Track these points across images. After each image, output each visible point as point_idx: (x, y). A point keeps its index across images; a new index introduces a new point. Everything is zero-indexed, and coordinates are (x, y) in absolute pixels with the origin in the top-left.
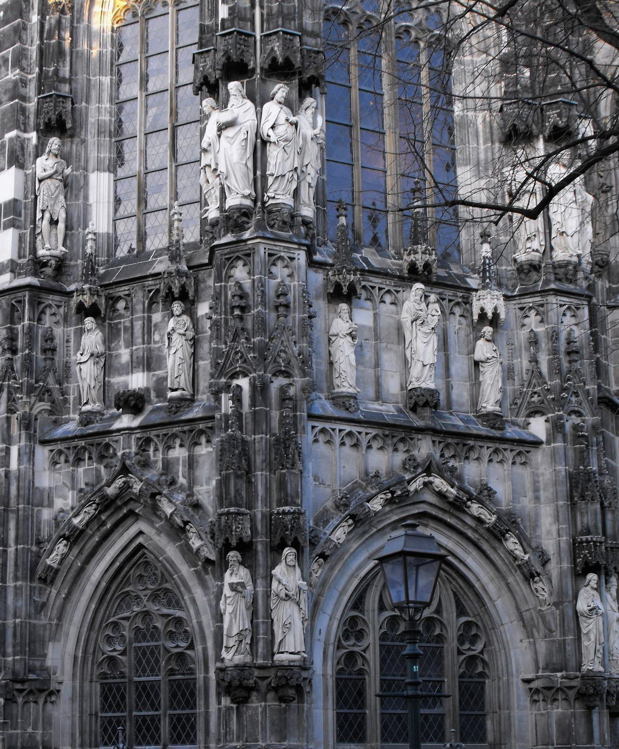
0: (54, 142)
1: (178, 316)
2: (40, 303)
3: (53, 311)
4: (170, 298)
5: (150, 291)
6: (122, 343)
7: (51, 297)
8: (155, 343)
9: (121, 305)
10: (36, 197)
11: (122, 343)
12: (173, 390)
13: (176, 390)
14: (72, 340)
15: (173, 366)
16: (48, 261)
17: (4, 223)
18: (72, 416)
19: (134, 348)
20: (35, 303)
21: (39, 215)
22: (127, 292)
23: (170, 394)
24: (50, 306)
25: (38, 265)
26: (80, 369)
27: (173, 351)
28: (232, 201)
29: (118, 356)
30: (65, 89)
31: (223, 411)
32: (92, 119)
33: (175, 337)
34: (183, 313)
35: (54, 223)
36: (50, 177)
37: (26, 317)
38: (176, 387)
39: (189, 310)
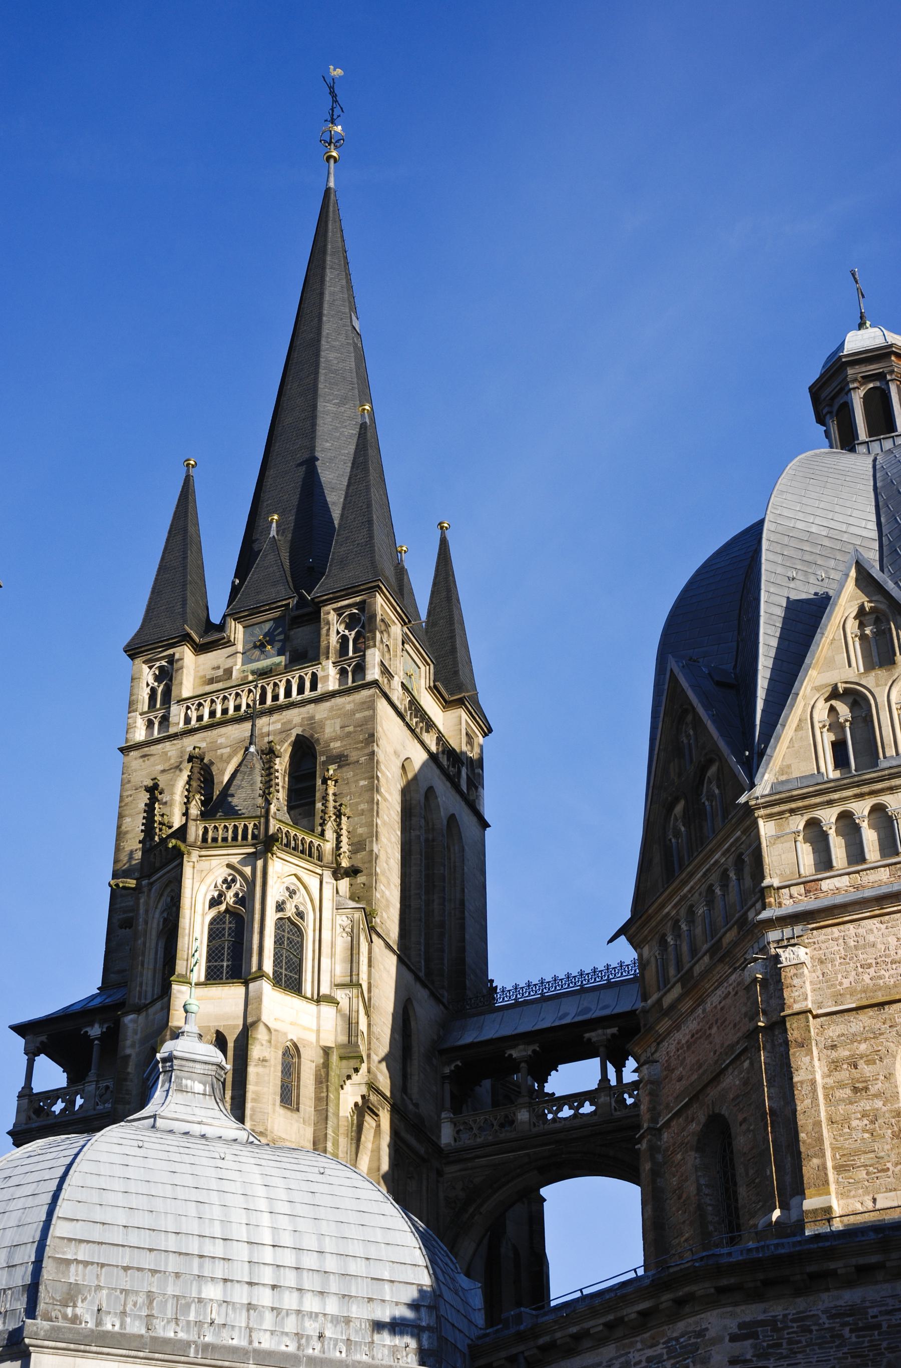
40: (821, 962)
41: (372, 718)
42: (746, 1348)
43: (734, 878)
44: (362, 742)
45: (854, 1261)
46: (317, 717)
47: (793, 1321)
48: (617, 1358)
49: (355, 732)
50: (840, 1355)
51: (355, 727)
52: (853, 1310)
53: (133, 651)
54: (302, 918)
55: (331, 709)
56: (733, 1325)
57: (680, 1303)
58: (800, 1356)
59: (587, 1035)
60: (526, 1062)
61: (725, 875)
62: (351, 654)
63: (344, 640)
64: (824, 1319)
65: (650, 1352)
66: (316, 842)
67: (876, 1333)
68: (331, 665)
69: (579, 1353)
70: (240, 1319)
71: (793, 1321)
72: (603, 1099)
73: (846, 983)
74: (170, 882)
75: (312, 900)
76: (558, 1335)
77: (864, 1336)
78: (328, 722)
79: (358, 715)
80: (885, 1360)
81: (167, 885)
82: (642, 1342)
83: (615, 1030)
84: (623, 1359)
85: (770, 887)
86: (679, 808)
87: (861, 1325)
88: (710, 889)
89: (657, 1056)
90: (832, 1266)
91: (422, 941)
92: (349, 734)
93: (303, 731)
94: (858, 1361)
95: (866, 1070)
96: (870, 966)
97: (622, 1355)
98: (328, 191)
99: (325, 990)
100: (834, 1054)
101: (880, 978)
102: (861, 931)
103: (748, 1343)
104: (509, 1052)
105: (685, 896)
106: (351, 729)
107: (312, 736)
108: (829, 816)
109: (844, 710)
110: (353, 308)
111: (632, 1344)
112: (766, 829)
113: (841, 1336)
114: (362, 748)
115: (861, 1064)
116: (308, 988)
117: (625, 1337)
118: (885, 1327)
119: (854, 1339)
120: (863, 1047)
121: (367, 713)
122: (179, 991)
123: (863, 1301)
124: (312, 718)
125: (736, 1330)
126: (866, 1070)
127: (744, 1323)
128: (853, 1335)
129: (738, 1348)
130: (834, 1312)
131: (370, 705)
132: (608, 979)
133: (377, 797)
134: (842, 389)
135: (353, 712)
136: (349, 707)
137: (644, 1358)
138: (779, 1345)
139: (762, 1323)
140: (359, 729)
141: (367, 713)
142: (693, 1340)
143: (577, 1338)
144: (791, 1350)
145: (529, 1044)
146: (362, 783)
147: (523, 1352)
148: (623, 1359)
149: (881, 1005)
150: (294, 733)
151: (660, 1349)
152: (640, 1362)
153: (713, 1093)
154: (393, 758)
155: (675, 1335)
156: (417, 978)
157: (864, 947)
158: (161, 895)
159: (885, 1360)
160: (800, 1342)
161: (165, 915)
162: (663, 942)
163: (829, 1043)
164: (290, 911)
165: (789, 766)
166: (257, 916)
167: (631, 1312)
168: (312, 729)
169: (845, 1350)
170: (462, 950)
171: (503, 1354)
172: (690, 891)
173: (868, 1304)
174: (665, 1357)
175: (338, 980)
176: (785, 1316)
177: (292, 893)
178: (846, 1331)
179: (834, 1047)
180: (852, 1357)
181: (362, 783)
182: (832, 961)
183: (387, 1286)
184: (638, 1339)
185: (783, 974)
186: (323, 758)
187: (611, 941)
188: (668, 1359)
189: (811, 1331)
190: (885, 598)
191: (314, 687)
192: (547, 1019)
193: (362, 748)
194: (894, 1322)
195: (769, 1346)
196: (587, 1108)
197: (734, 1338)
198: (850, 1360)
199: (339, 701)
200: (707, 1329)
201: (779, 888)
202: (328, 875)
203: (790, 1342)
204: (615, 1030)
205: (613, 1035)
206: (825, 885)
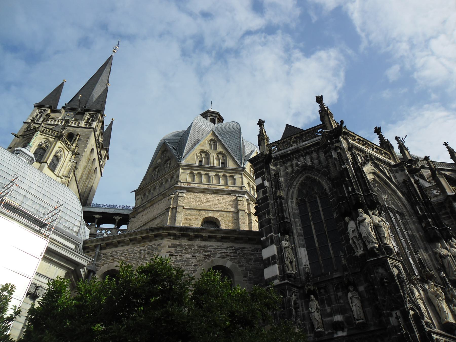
0: (287, 237)
1: (352, 291)
2: (291, 290)
3: (295, 294)
4: (349, 284)
5: (335, 285)
6: (326, 305)
7: (294, 288)
8: (341, 303)
9: (322, 291)
10: (283, 254)
11: (326, 305)
12: (357, 320)
13: (360, 320)
14: (304, 305)
15: (356, 310)
16: (292, 275)
17: (272, 263)
18: (309, 335)
19: (333, 306)
20: (290, 290)
21: (286, 260)
22: (325, 286)
23: (357, 322)
24: (294, 292)
25: (289, 276)
26: (312, 315)
27: (354, 304)
28: (370, 246)
29: (326, 310)
30: (286, 220)
31: (392, 324)
32: (295, 232)
33: (354, 299)
34: (354, 290)
35: (291, 262)
36: (288, 247)
37: (288, 295)
38: (360, 318)
39: (356, 289)
40: (188, 198)
41: (90, 134)
42: (173, 250)
43: (169, 181)
45: (208, 234)
46: (77, 130)
47: (187, 246)
48: (130, 249)
50: (199, 256)
52: (204, 246)
53: (36, 106)
54: (61, 158)
55: (81, 130)
56: (170, 244)
57: (156, 236)
58: (187, 254)
59: (114, 217)
60: (97, 219)
61: (167, 180)
62: (90, 122)
63: (89, 119)
64: (196, 247)
65: (141, 248)
66: (70, 145)
67: (210, 253)
68: (84, 122)
69: (118, 247)
70: (20, 198)
71: (187, 246)
72: (114, 231)
73: (193, 204)
74: (29, 138)
76: (114, 240)
77: (207, 253)
79: (87, 133)
80: (211, 260)
81: (27, 139)
82: (139, 246)
83: (121, 218)
84: (132, 249)
85: (180, 181)
86: (157, 170)
87: (206, 250)
88: (162, 184)
89: (135, 217)
90: (202, 234)
91: (82, 186)
94: (204, 258)
95: (194, 222)
96: (199, 202)
97: (132, 248)
98: (112, 56)
99: (60, 175)
100: (186, 217)
101: (201, 205)
102: (198, 195)
103: (173, 249)
104: (94, 216)
105: (154, 184)
107: (74, 133)
108: (196, 172)
109: (203, 155)
110: (110, 74)
111: (136, 246)
112: (181, 171)
113: (200, 252)
115: (192, 221)
116: (56, 172)
117: (135, 244)
118: (212, 252)
119: (203, 253)
120: (194, 217)
121: (89, 133)
123: (208, 245)
124: (76, 130)
125: (171, 245)
126: (194, 222)
127: (173, 244)
128: (203, 252)
129: (169, 249)
130: (199, 246)
131: (91, 132)
132: (122, 208)
133: (85, 149)
134: (207, 116)
135: (86, 132)
136: (85, 131)
137: (139, 249)
138: (183, 251)
139: (178, 245)
141: (89, 133)
142: (156, 246)
143: (119, 242)
144: (185, 252)
145: (99, 215)
146: (83, 145)
147: (100, 244)
148: (132, 249)
149: (200, 210)
150: (70, 132)
151: (145, 248)
152: (138, 250)
153: (150, 223)
154: (91, 146)
155: (151, 244)
156: (79, 192)
157: (198, 198)
158: (25, 140)
159: (211, 260)
160: (188, 251)
161: (24, 145)
162: (145, 195)
163: (186, 214)
164: (59, 154)
165: (189, 161)
166: (50, 151)
167: (139, 237)
169: (201, 255)
170: (89, 195)
171: (94, 244)
172: (156, 184)
173: (209, 246)
174: (146, 249)
175: (64, 175)
176: (185, 244)
177: (61, 152)
178: (201, 251)
179: (187, 215)
180: (202, 257)
181: (83, 145)
182: (191, 199)
183: (69, 211)
184: (139, 245)
185: (179, 198)
187: (131, 192)
188: (147, 250)
189: (192, 249)
190: (217, 138)
191: (78, 125)
192: (107, 211)
194: (215, 251)
195: (179, 250)
196: (109, 232)
197: (169, 247)
198: (201, 258)
199: (84, 129)
200: (162, 244)
201: (182, 182)
202: (70, 153)
203: (185, 250)
204: (121, 218)
205: (121, 218)
206: (192, 185)
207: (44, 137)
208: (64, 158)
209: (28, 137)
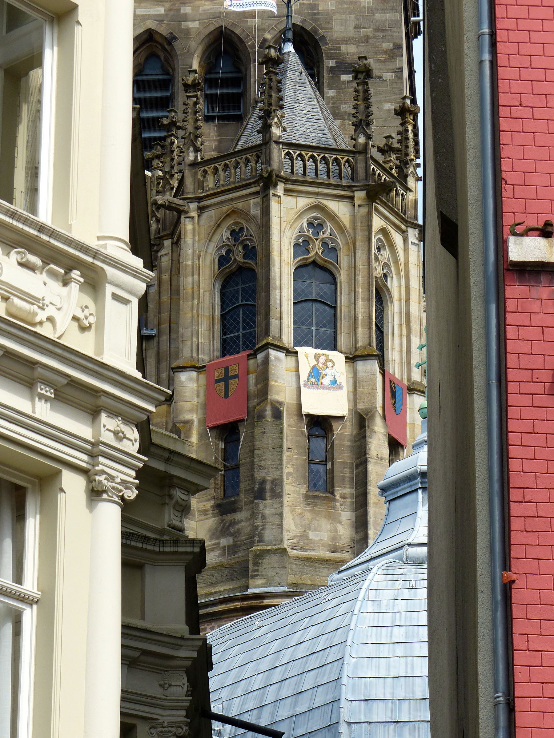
44: (385, 52)
49: (375, 37)
51: (375, 31)
75: (396, 262)
78: (337, 17)
79: (377, 16)
92: (366, 40)
93: (304, 21)
106: (369, 32)
107: (316, 31)
114: (385, 61)
122: (277, 358)
140: (381, 35)
161: (223, 252)
168: (315, 20)
186: (331, 63)
193: (385, 61)
207: (303, 202)
208: (398, 274)
209: (226, 208)
